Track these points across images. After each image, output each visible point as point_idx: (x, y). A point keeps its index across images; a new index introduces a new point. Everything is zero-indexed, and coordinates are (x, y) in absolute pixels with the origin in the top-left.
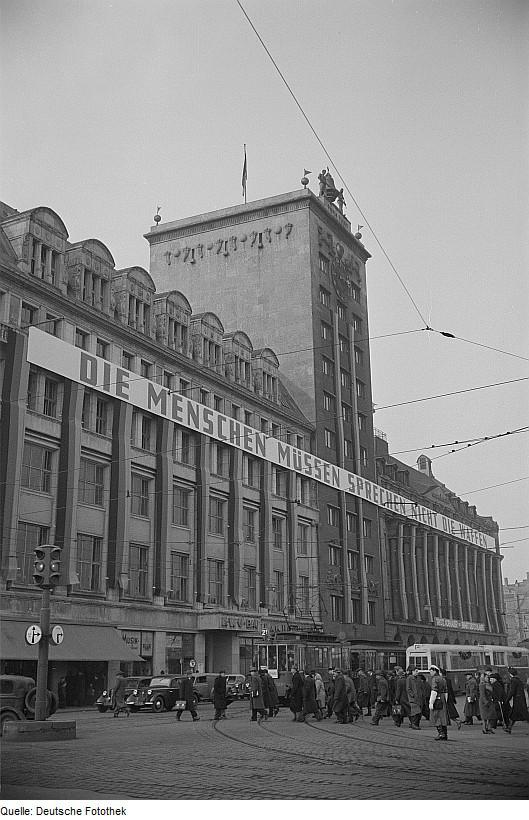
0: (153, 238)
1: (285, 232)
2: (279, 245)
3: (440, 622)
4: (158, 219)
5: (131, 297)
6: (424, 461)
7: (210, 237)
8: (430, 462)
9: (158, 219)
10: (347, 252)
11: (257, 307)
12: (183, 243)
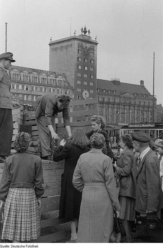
0: (50, 45)
1: (70, 46)
2: (69, 49)
3: (119, 124)
4: (51, 40)
5: (24, 76)
6: (142, 82)
7: (59, 46)
8: (143, 82)
9: (51, 40)
10: (88, 45)
11: (66, 62)
12: (55, 46)
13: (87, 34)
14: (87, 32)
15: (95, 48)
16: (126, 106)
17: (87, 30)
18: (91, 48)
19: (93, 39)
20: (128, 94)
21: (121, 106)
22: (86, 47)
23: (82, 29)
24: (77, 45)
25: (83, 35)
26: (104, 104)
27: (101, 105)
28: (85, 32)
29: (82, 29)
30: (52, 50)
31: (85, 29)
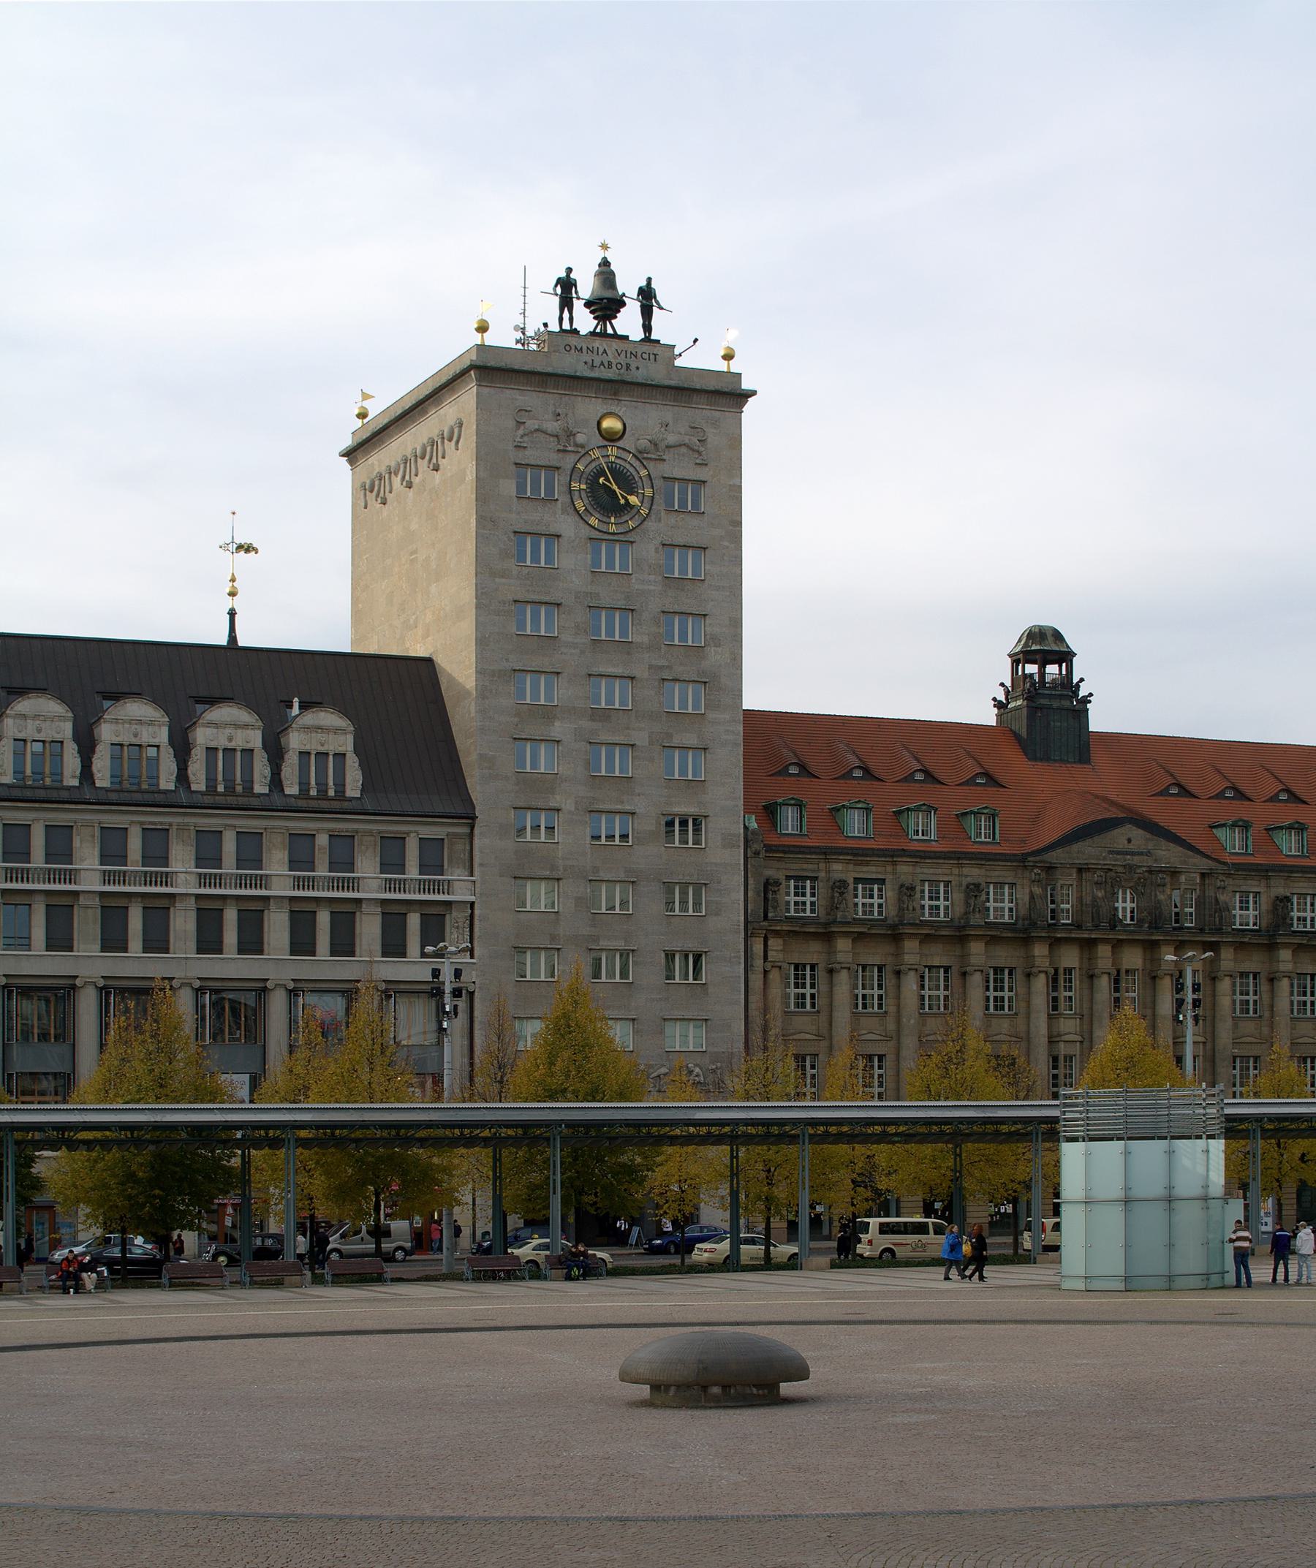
10: (643, 421)
13: (628, 322)
14: (618, 303)
15: (713, 438)
16: (1104, 951)
17: (628, 285)
18: (672, 439)
19: (700, 358)
20: (1138, 837)
21: (1040, 951)
22: (611, 438)
23: (566, 286)
24: (511, 424)
25: (575, 332)
26: (843, 945)
27: (812, 953)
28: (607, 306)
29: (559, 281)
30: (371, 492)
31: (606, 274)
